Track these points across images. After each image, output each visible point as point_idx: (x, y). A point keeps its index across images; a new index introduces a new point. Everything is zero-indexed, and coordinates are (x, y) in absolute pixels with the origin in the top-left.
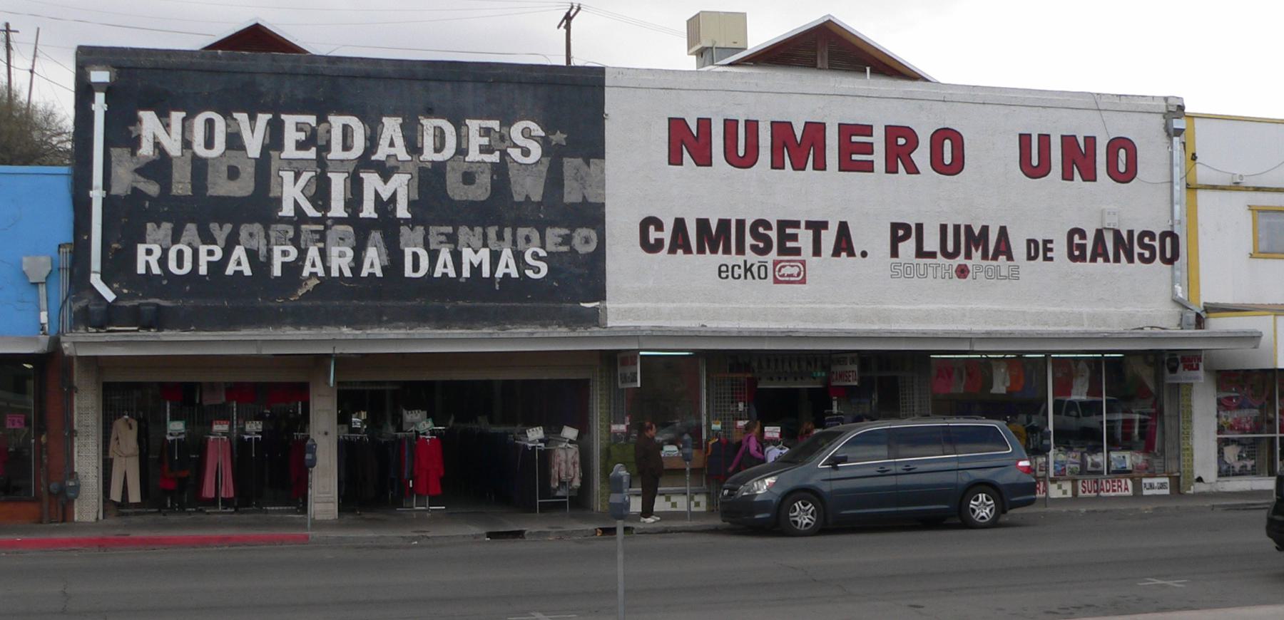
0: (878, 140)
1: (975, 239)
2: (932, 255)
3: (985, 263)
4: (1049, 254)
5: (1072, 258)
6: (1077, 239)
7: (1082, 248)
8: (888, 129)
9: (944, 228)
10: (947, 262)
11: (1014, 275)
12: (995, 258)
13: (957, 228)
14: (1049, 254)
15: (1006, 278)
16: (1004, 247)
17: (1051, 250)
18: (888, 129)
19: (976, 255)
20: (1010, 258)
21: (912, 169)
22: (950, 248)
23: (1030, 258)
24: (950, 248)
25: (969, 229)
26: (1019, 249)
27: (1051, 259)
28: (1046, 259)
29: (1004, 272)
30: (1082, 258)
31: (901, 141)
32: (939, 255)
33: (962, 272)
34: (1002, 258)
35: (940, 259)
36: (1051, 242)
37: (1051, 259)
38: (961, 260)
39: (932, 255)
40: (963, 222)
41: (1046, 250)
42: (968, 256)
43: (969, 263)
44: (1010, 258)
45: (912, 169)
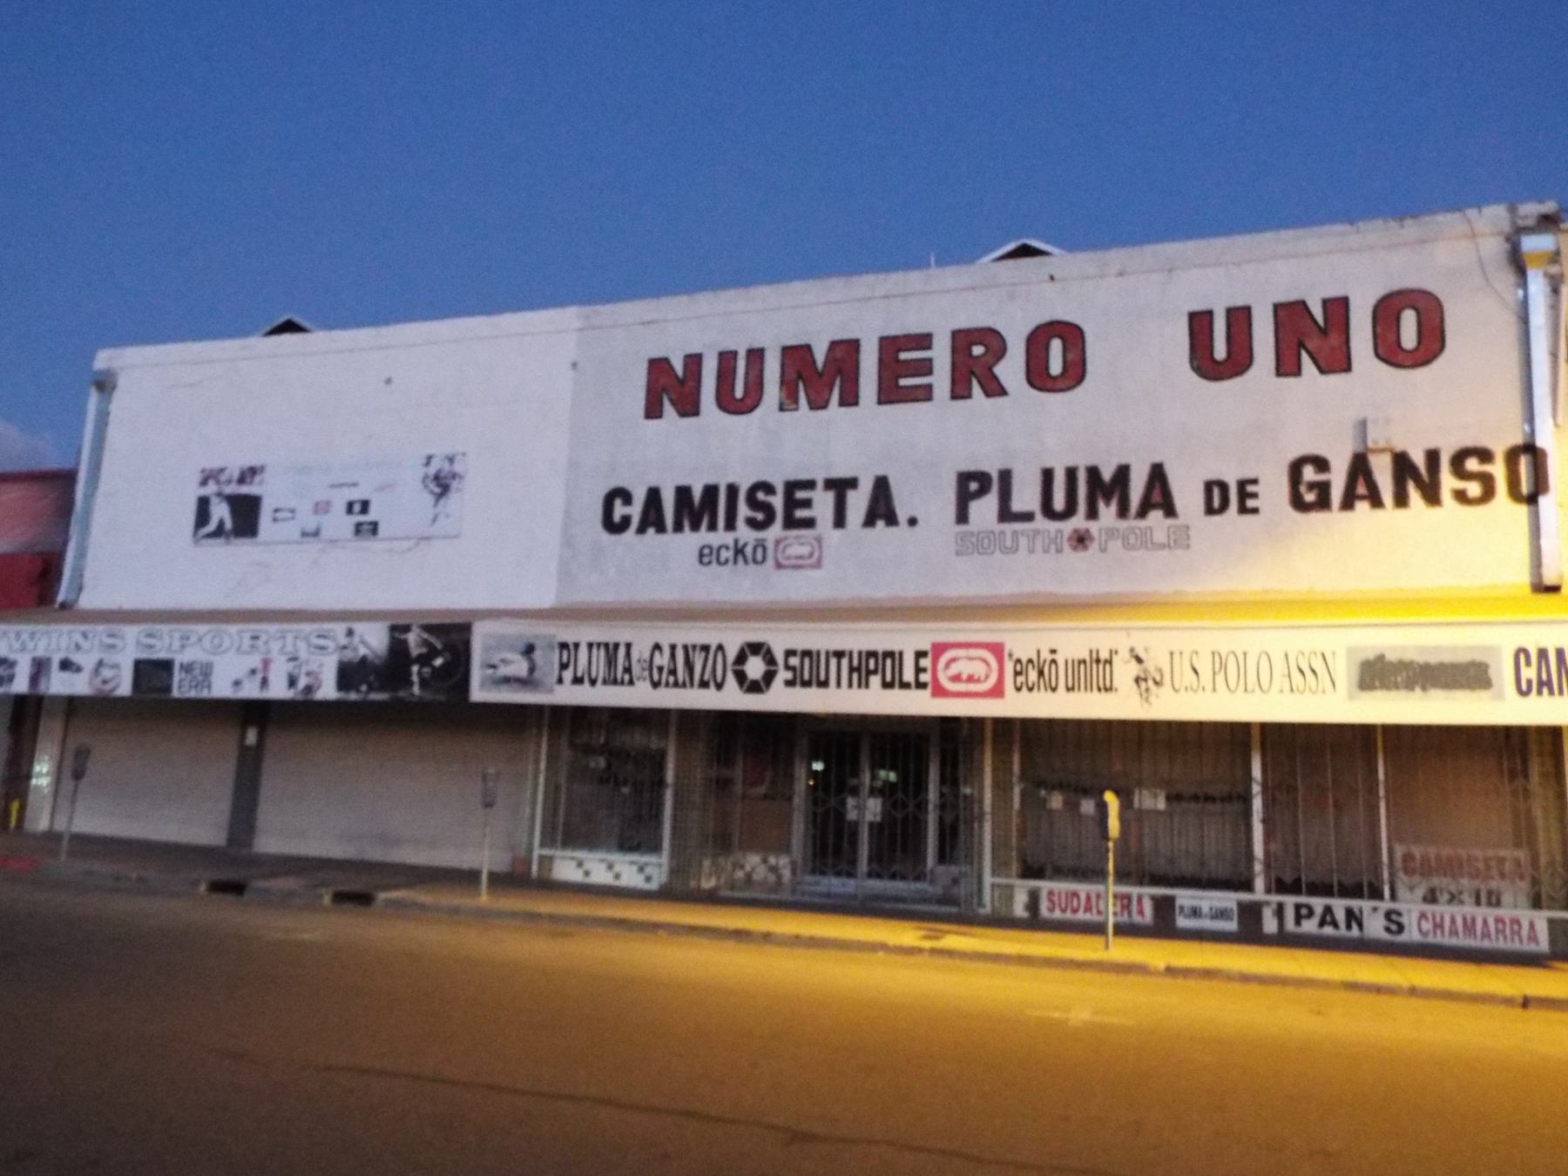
0: (941, 354)
1: (1106, 488)
2: (1028, 517)
3: (1123, 525)
4: (1250, 503)
5: (1298, 504)
6: (1309, 474)
7: (1323, 489)
8: (957, 335)
9: (1048, 475)
10: (1053, 526)
11: (1181, 540)
12: (1142, 513)
13: (1071, 474)
14: (1250, 503)
15: (1162, 546)
16: (1159, 494)
17: (1254, 495)
18: (957, 335)
19: (1108, 512)
20: (1170, 511)
21: (995, 389)
22: (1059, 503)
23: (1210, 510)
24: (1059, 503)
25: (1093, 472)
26: (1188, 496)
27: (1255, 511)
28: (1243, 510)
29: (1160, 537)
30: (1323, 503)
31: (978, 350)
32: (1039, 516)
33: (1081, 540)
34: (1156, 516)
35: (1041, 522)
36: (1255, 482)
37: (1255, 511)
38: (1078, 521)
39: (1028, 517)
40: (1082, 462)
41: (1243, 495)
42: (1092, 514)
43: (1093, 527)
44: (1170, 511)
45: (995, 389)
